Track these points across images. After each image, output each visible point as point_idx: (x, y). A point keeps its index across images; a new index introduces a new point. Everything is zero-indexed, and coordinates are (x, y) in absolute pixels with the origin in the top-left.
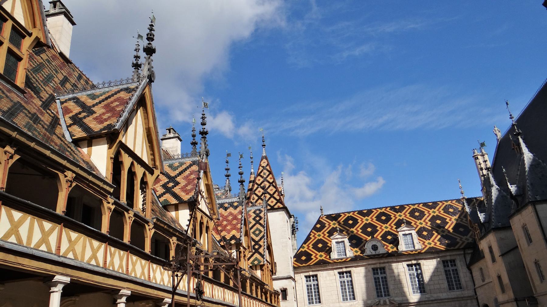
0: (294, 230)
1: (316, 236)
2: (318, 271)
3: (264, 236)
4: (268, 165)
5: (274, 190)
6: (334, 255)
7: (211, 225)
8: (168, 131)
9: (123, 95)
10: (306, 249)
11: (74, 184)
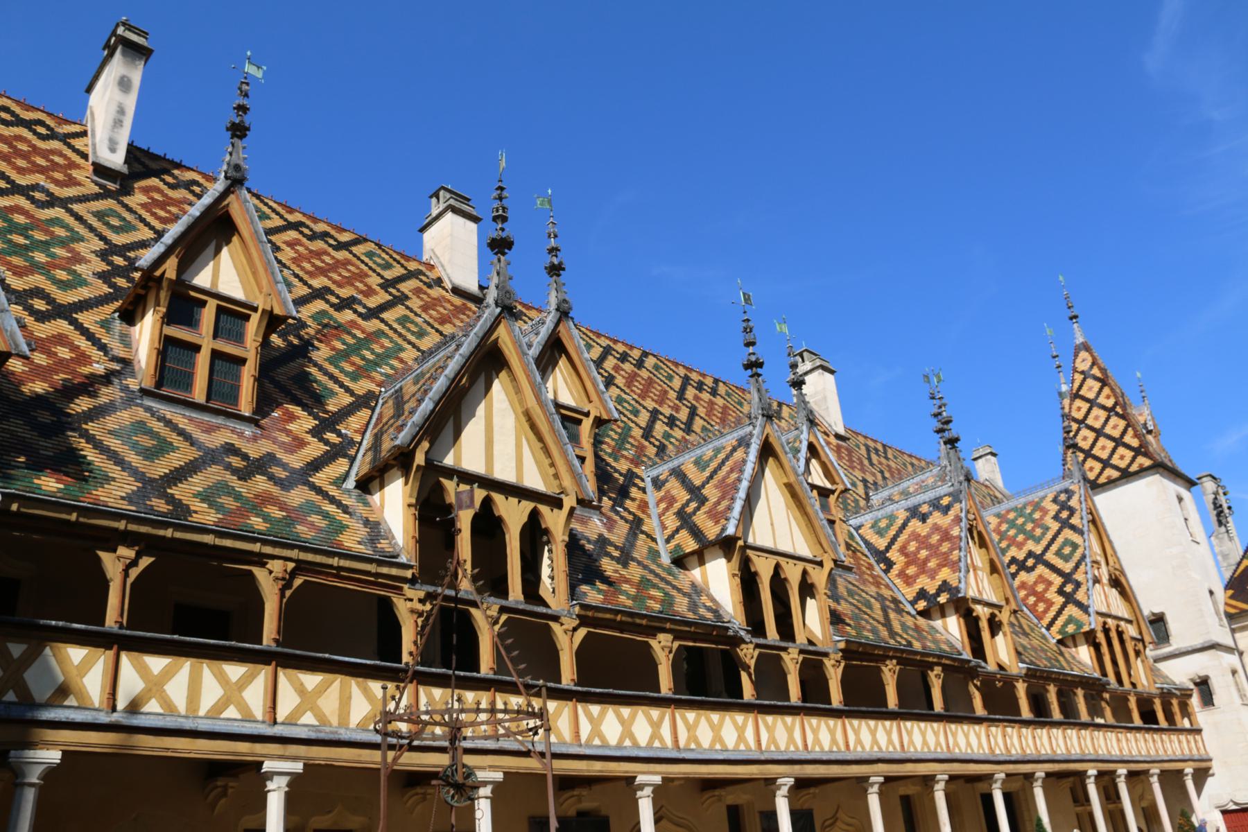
3: (1083, 557)
4: (1094, 364)
5: (1122, 424)
7: (819, 577)
11: (298, 582)
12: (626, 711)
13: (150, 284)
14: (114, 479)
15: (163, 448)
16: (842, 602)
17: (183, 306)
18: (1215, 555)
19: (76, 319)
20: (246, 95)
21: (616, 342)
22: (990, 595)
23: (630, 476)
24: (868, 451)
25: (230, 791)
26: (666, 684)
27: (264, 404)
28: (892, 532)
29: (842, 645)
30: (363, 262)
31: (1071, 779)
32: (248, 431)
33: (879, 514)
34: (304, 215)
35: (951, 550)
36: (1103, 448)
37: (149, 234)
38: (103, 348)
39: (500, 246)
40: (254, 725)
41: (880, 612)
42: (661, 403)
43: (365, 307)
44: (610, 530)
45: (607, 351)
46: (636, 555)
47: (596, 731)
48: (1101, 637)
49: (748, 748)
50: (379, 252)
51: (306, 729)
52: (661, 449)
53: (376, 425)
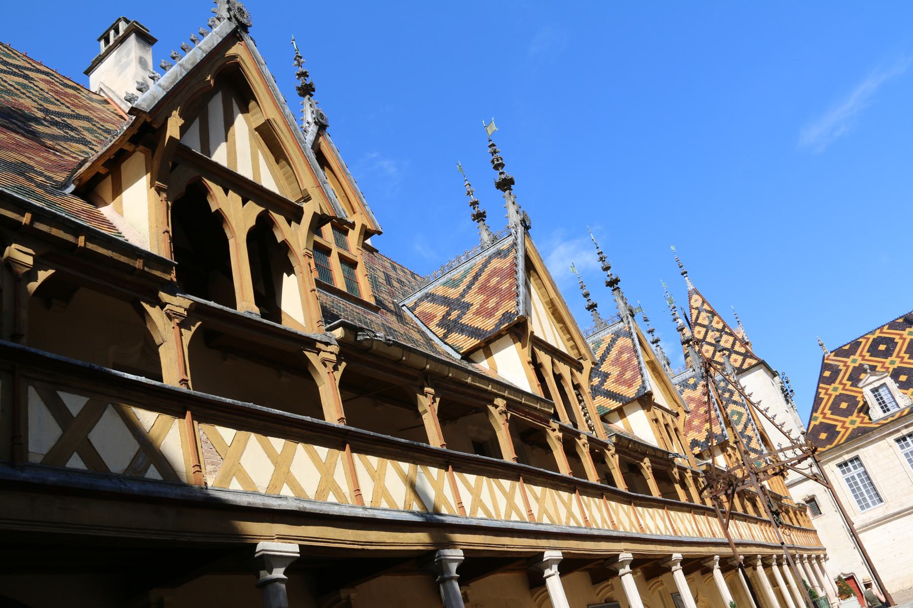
0: (787, 395)
1: (829, 392)
2: (858, 448)
4: (704, 302)
5: (731, 339)
6: (876, 413)
9: (496, 263)
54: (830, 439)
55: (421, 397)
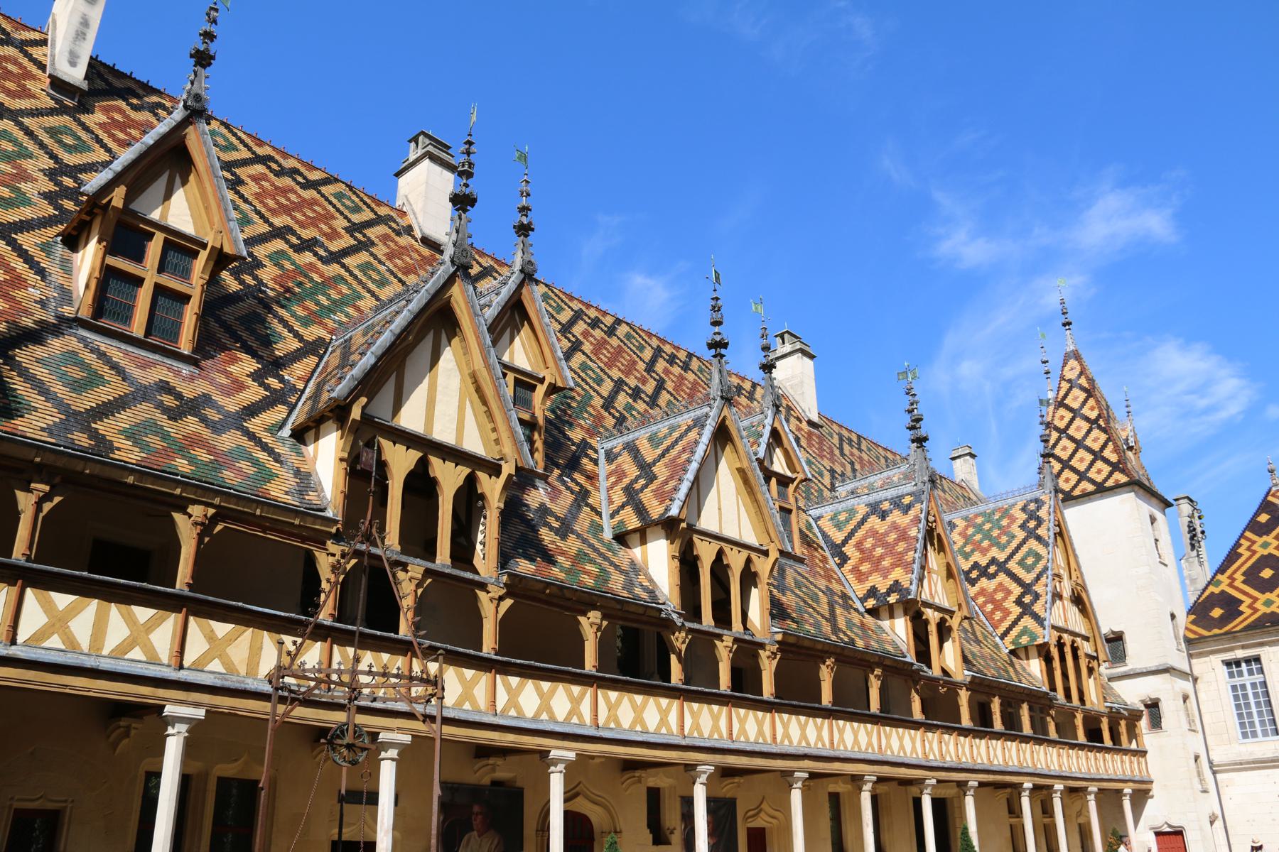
0: (1194, 538)
1: (1255, 547)
3: (1046, 569)
4: (1081, 373)
5: (1103, 437)
7: (763, 566)
8: (779, 339)
10: (1224, 587)
12: (546, 685)
13: (96, 211)
14: (36, 409)
15: (92, 380)
16: (788, 593)
17: (128, 236)
18: (1182, 578)
19: (15, 240)
20: (214, 22)
21: (589, 306)
22: (942, 600)
23: (584, 445)
24: (841, 440)
25: (133, 732)
26: (590, 662)
27: (207, 345)
28: (850, 527)
29: (779, 637)
30: (330, 203)
31: (1009, 790)
32: (186, 370)
33: (840, 507)
34: (274, 149)
35: (907, 550)
36: (1082, 460)
37: (104, 156)
38: (42, 272)
39: (462, 202)
40: (158, 668)
41: (826, 607)
42: (627, 374)
43: (326, 250)
44: (553, 500)
45: (578, 316)
46: (576, 527)
47: (513, 702)
48: (1055, 652)
49: (670, 731)
50: (350, 194)
51: (212, 676)
52: (621, 420)
53: (321, 373)
54: (1223, 621)
55: (20, 495)
